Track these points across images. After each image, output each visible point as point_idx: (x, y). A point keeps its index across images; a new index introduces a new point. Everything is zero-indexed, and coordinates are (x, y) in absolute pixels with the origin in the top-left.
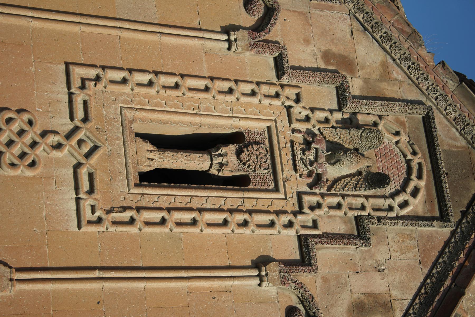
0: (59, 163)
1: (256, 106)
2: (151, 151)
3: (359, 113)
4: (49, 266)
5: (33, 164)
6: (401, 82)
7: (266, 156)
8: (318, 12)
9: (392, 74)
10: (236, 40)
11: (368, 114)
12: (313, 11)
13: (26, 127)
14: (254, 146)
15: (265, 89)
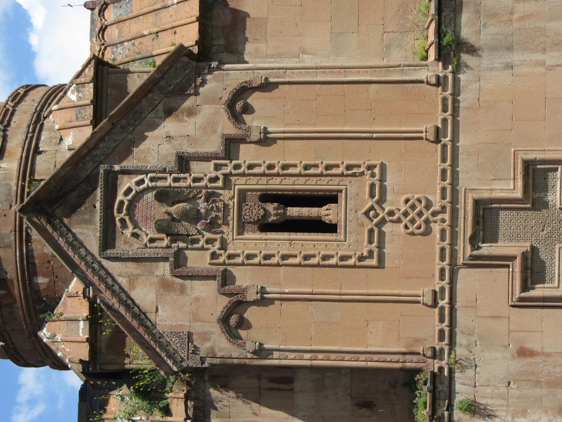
0: (392, 203)
1: (247, 248)
2: (327, 215)
3: (164, 248)
4: (403, 141)
5: (407, 201)
6: (120, 275)
7: (245, 214)
8: (183, 323)
9: (127, 281)
10: (257, 293)
11: (157, 247)
12: (187, 324)
13: (409, 225)
14: (252, 220)
15: (239, 260)
